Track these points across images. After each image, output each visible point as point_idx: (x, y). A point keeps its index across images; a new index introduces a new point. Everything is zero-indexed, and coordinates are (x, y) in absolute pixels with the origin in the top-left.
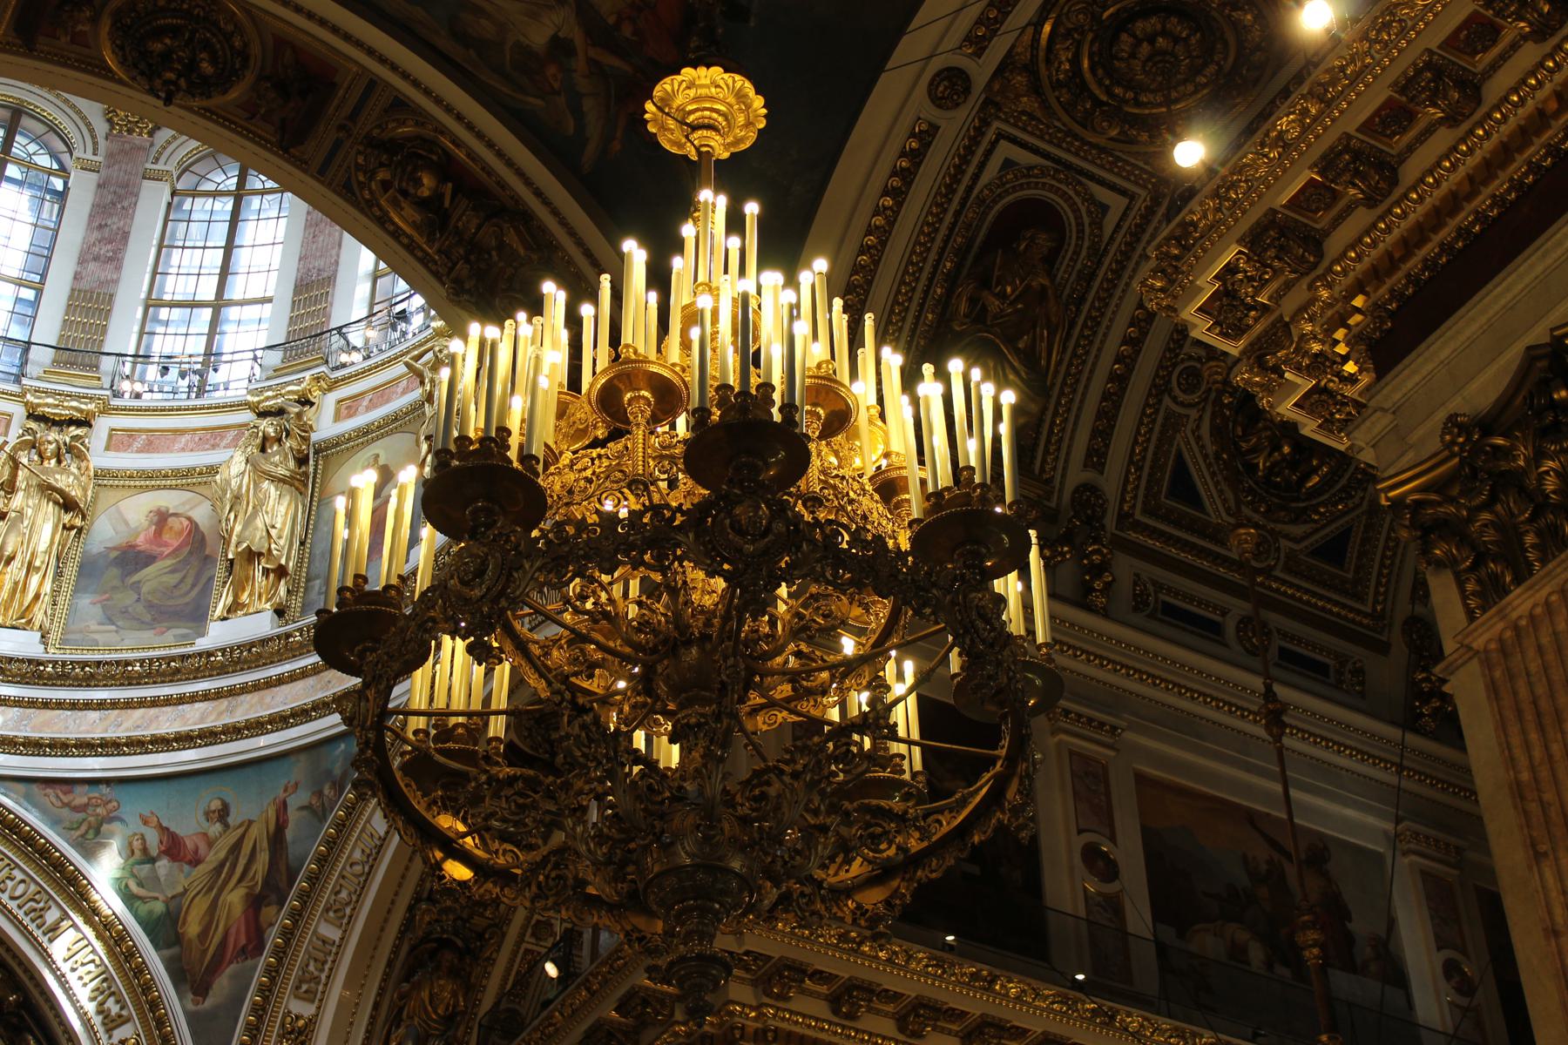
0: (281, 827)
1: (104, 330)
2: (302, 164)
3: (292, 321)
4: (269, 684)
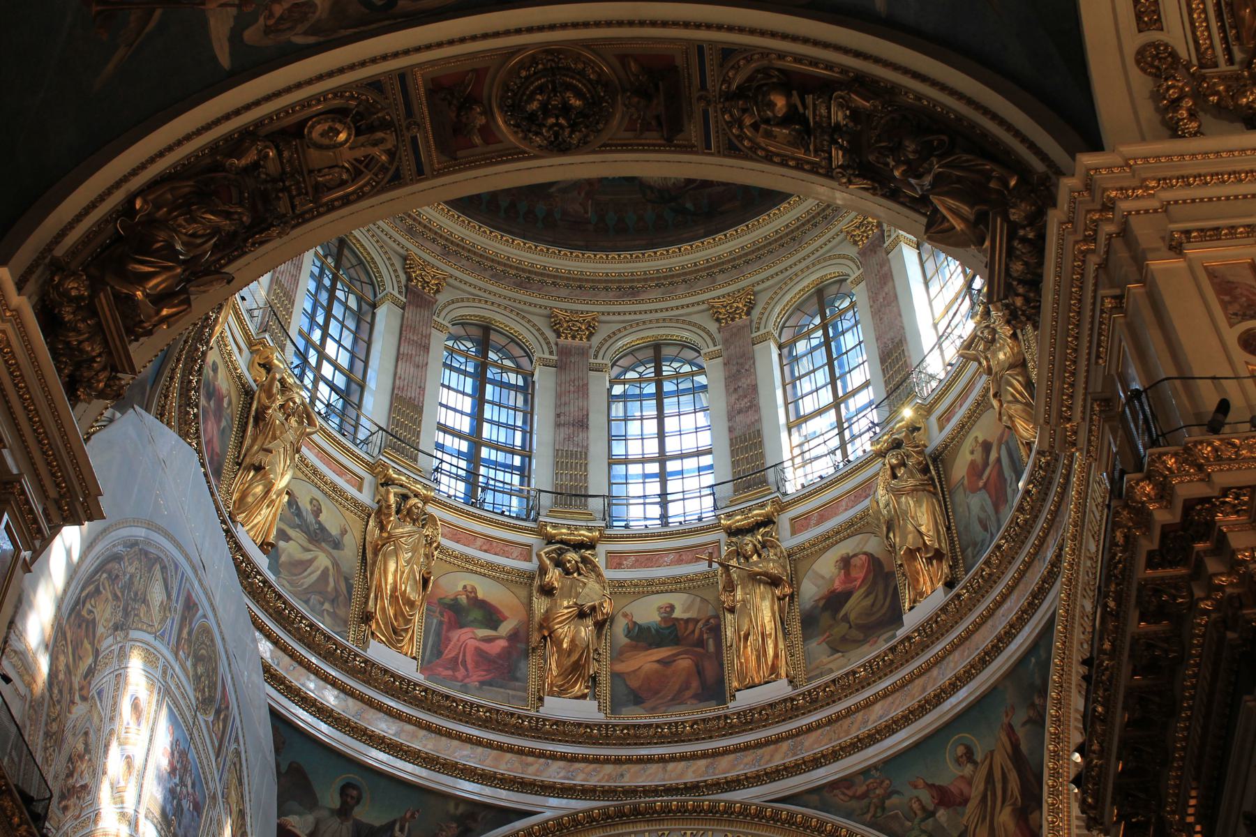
0: (1015, 746)
1: (762, 455)
2: (688, 149)
3: (887, 383)
4: (962, 640)
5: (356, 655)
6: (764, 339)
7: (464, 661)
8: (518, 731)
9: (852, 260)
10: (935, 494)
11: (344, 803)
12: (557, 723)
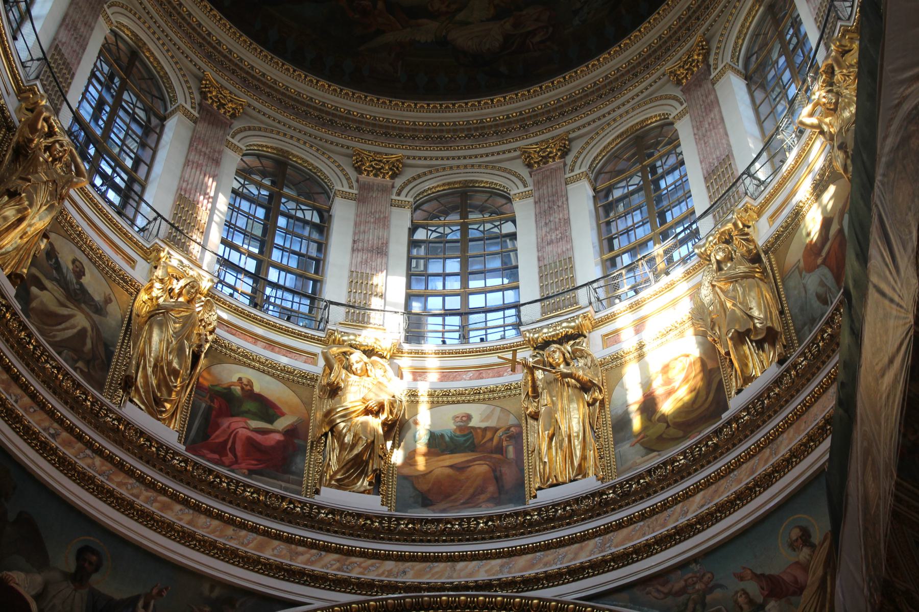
1: (573, 279)
4: (798, 415)
5: (110, 410)
6: (577, 179)
7: (233, 450)
8: (288, 517)
9: (675, 98)
10: (769, 283)
11: (80, 568)
12: (333, 511)
